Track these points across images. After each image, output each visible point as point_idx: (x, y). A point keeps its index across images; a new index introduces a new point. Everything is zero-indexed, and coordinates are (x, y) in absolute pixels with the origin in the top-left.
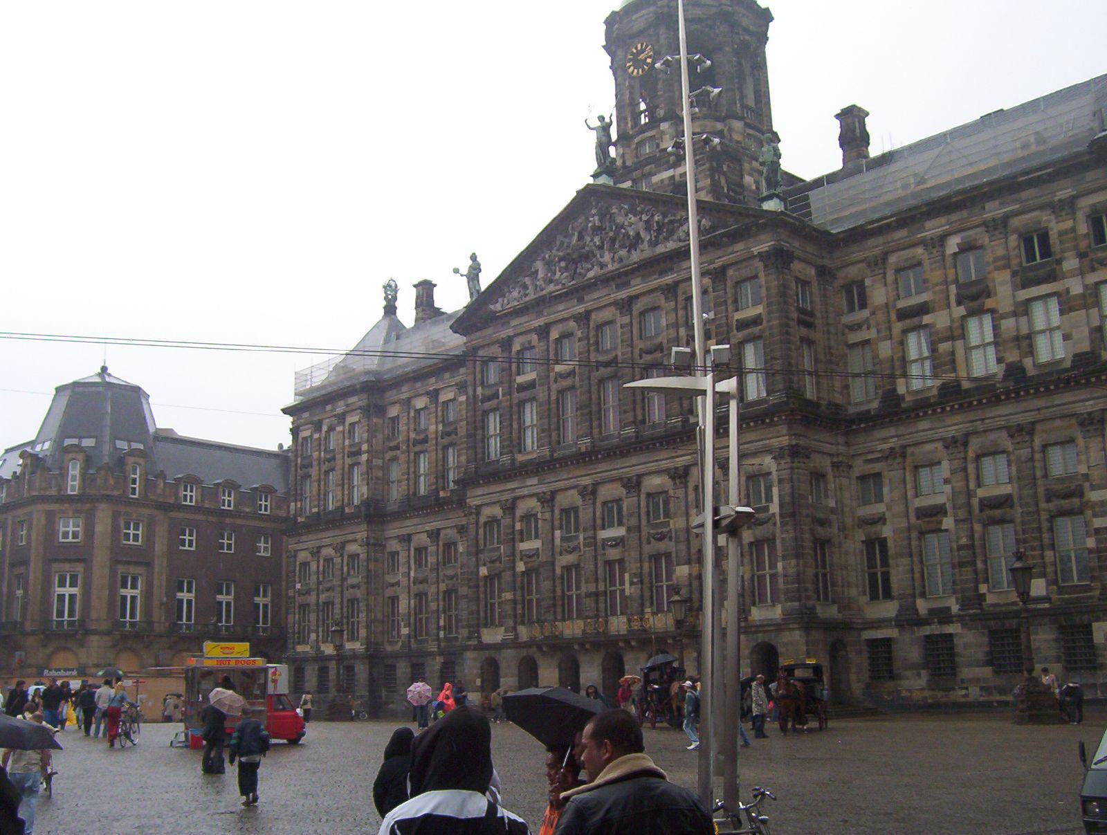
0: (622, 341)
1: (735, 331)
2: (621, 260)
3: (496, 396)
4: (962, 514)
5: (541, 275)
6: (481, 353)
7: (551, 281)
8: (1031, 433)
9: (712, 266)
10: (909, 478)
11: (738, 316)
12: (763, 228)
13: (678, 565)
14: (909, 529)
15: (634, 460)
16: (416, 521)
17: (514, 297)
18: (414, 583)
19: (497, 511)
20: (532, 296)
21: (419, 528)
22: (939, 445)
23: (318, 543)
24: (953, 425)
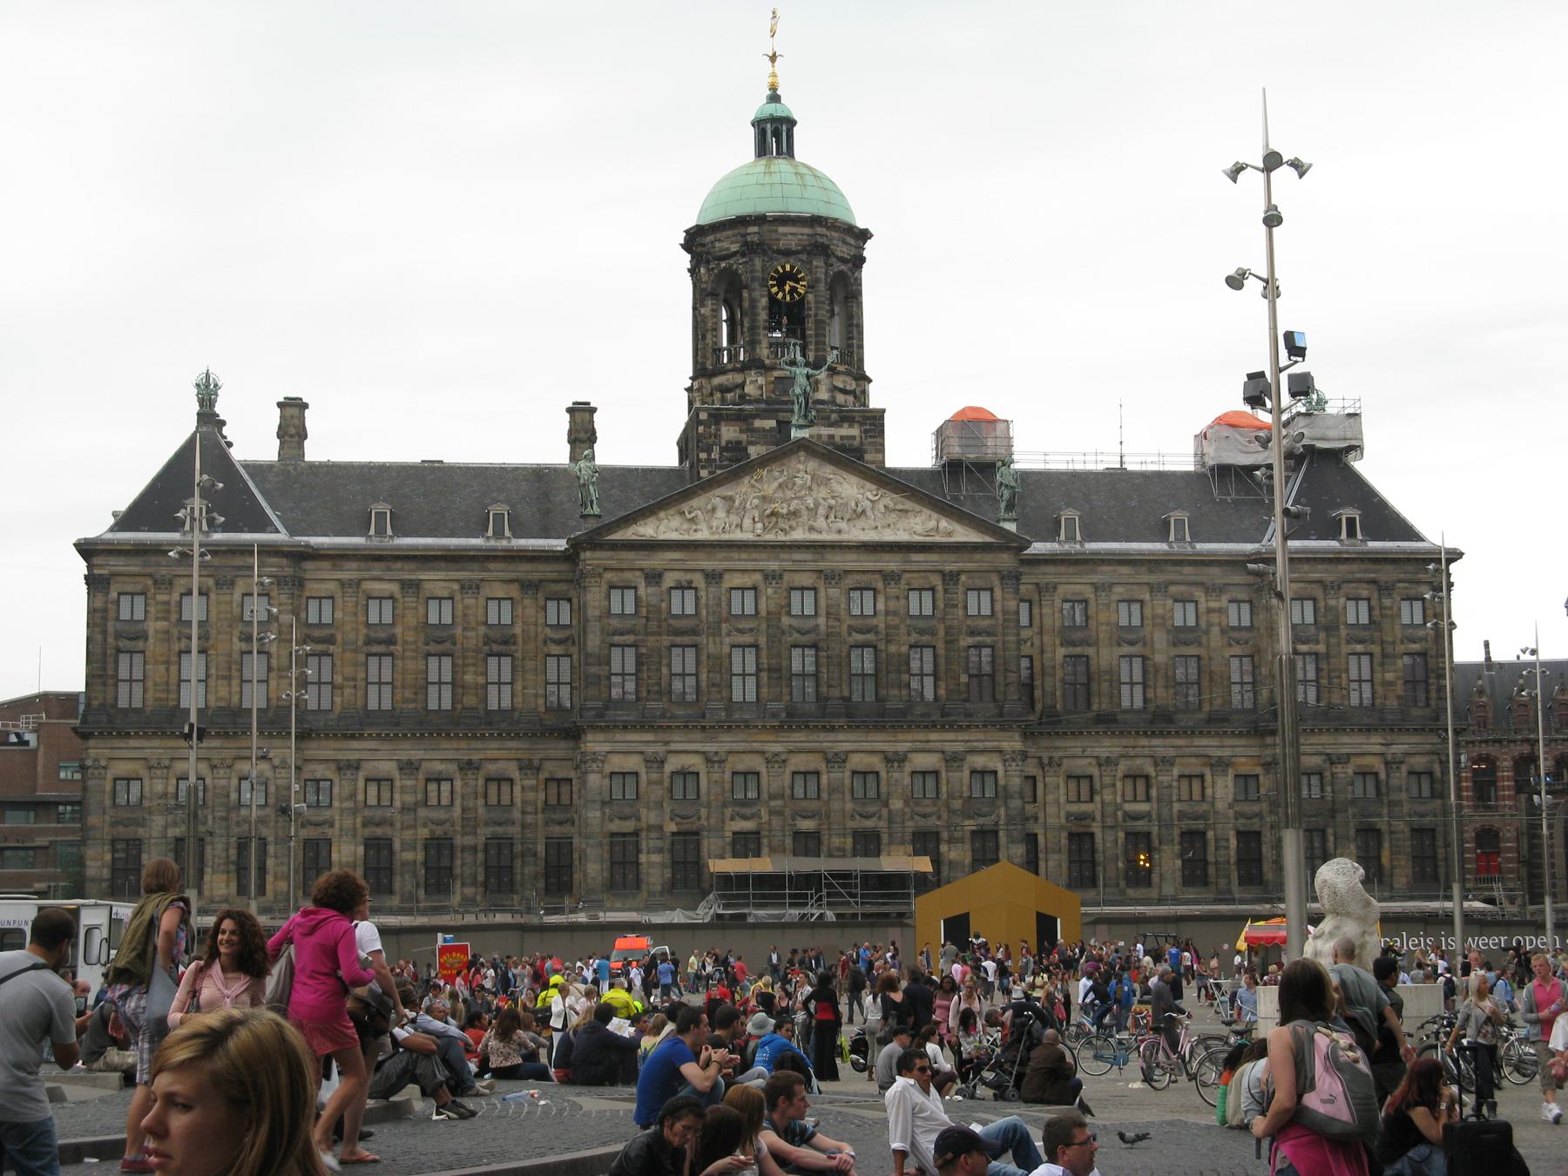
0: (828, 613)
2: (840, 532)
4: (1109, 822)
5: (721, 514)
6: (608, 576)
8: (1172, 764)
9: (948, 568)
10: (1062, 786)
12: (1008, 548)
13: (890, 843)
14: (1062, 828)
15: (841, 737)
16: (373, 744)
18: (364, 825)
19: (632, 763)
20: (703, 535)
21: (382, 759)
22: (1094, 761)
23: (170, 753)
24: (1107, 747)
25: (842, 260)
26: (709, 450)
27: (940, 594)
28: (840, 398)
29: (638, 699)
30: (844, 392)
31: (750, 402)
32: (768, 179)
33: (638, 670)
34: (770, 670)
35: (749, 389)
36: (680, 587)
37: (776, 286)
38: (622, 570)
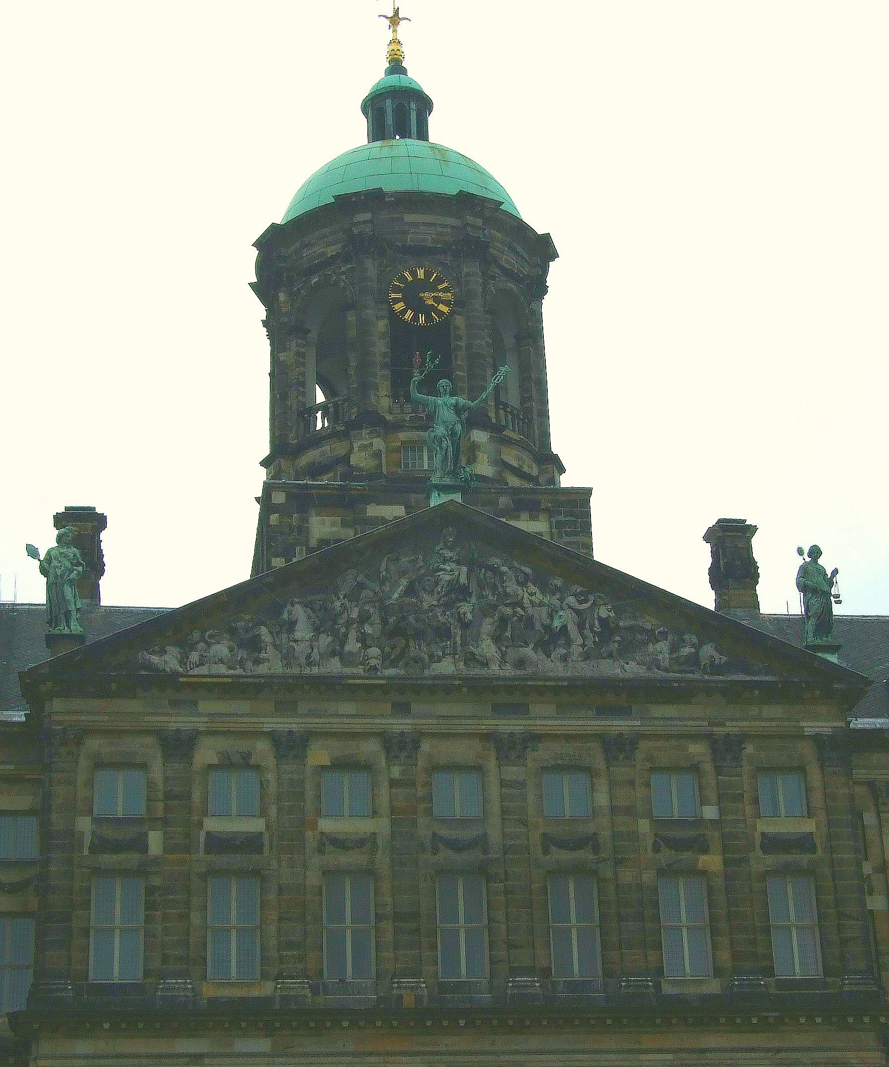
0: (504, 811)
1: (759, 853)
2: (521, 663)
3: (140, 844)
5: (303, 631)
6: (94, 744)
7: (333, 654)
11: (764, 826)
17: (218, 656)
20: (272, 665)
25: (510, 274)
26: (287, 553)
27: (710, 778)
28: (514, 481)
29: (147, 973)
30: (518, 472)
31: (359, 479)
32: (386, 152)
33: (148, 919)
34: (397, 917)
35: (359, 459)
36: (226, 764)
37: (403, 299)
38: (120, 733)
